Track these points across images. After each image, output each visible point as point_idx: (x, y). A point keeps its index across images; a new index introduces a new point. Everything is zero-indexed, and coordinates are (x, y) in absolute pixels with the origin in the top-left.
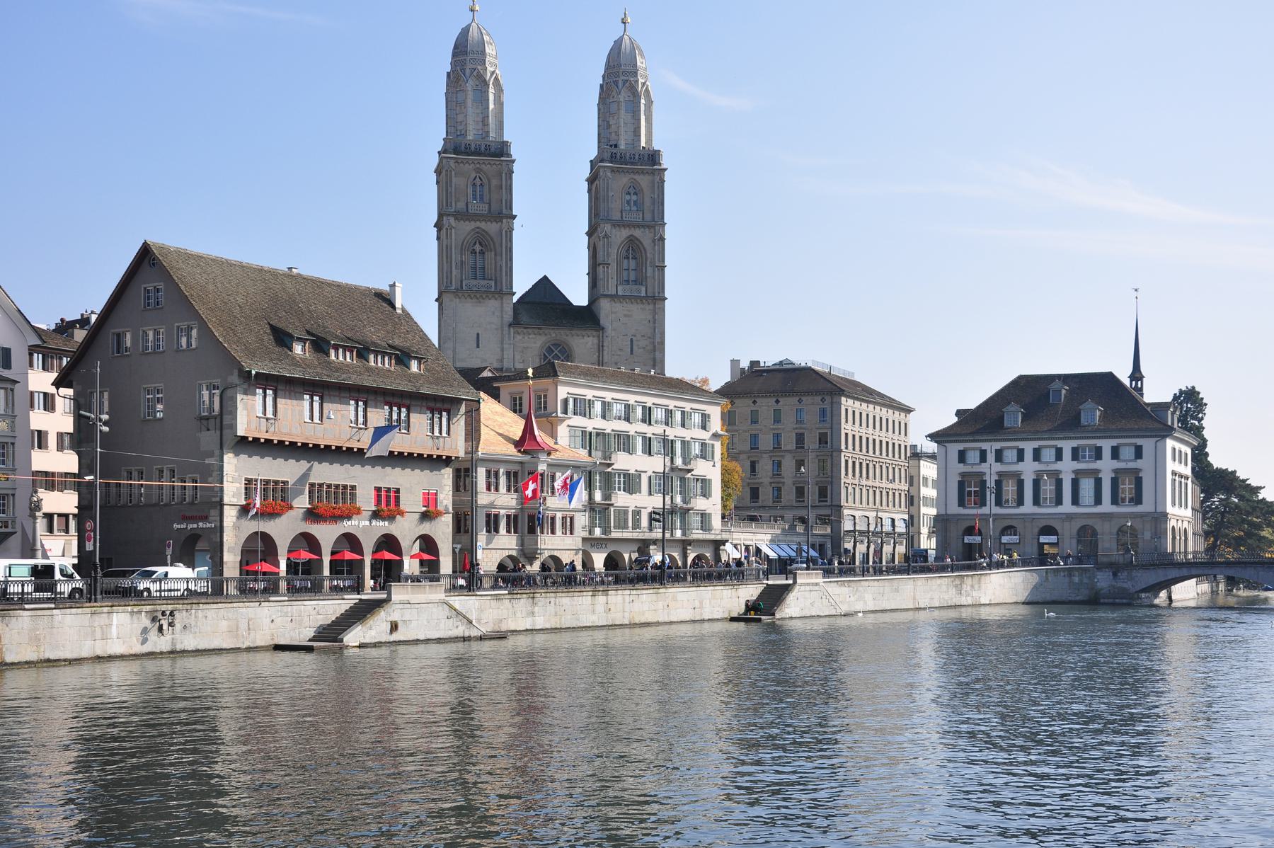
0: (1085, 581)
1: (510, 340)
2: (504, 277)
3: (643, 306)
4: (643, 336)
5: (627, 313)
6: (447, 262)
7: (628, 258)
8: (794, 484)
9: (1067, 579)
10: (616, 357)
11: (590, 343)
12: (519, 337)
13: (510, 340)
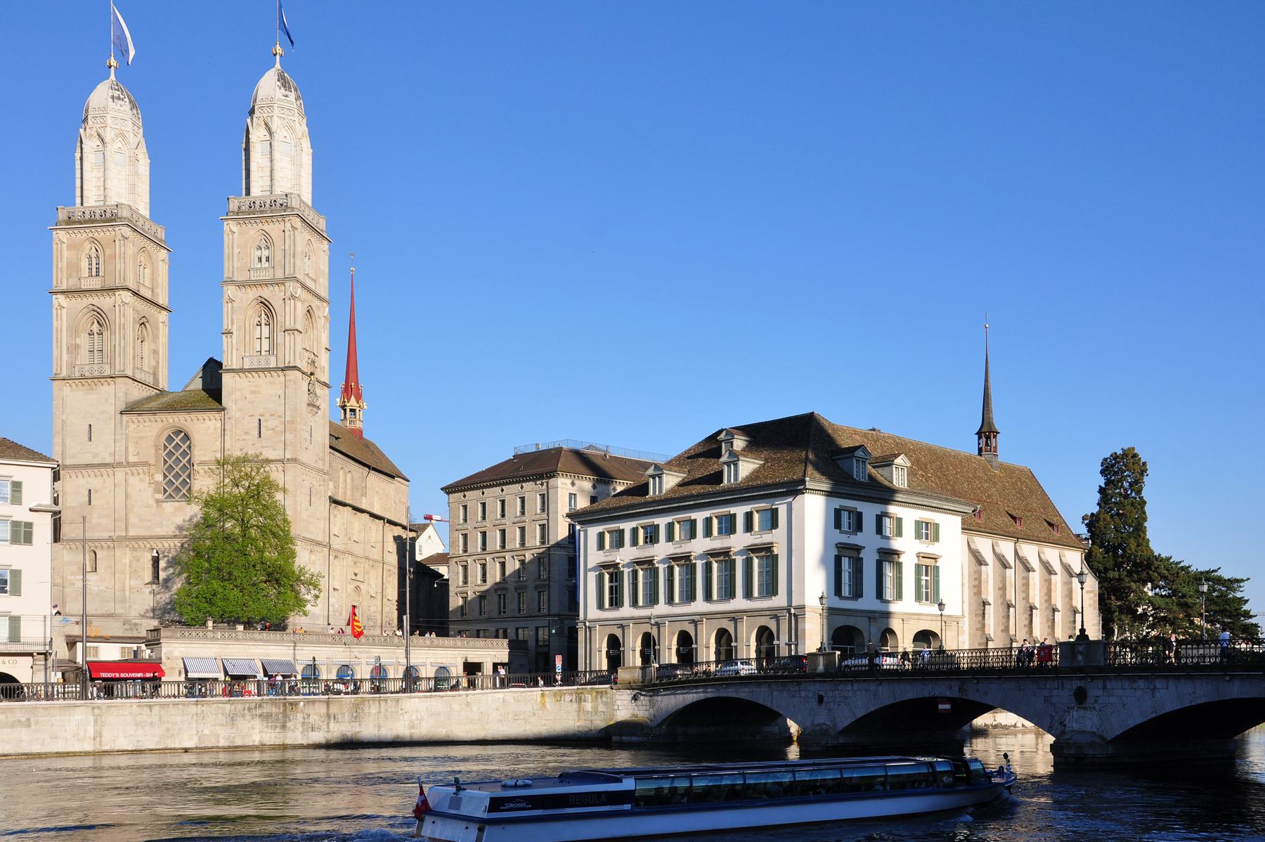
0: (601, 708)
1: (122, 429)
3: (272, 380)
4: (273, 415)
5: (254, 389)
6: (57, 347)
7: (261, 325)
10: (242, 442)
11: (212, 428)
12: (133, 426)
13: (122, 429)
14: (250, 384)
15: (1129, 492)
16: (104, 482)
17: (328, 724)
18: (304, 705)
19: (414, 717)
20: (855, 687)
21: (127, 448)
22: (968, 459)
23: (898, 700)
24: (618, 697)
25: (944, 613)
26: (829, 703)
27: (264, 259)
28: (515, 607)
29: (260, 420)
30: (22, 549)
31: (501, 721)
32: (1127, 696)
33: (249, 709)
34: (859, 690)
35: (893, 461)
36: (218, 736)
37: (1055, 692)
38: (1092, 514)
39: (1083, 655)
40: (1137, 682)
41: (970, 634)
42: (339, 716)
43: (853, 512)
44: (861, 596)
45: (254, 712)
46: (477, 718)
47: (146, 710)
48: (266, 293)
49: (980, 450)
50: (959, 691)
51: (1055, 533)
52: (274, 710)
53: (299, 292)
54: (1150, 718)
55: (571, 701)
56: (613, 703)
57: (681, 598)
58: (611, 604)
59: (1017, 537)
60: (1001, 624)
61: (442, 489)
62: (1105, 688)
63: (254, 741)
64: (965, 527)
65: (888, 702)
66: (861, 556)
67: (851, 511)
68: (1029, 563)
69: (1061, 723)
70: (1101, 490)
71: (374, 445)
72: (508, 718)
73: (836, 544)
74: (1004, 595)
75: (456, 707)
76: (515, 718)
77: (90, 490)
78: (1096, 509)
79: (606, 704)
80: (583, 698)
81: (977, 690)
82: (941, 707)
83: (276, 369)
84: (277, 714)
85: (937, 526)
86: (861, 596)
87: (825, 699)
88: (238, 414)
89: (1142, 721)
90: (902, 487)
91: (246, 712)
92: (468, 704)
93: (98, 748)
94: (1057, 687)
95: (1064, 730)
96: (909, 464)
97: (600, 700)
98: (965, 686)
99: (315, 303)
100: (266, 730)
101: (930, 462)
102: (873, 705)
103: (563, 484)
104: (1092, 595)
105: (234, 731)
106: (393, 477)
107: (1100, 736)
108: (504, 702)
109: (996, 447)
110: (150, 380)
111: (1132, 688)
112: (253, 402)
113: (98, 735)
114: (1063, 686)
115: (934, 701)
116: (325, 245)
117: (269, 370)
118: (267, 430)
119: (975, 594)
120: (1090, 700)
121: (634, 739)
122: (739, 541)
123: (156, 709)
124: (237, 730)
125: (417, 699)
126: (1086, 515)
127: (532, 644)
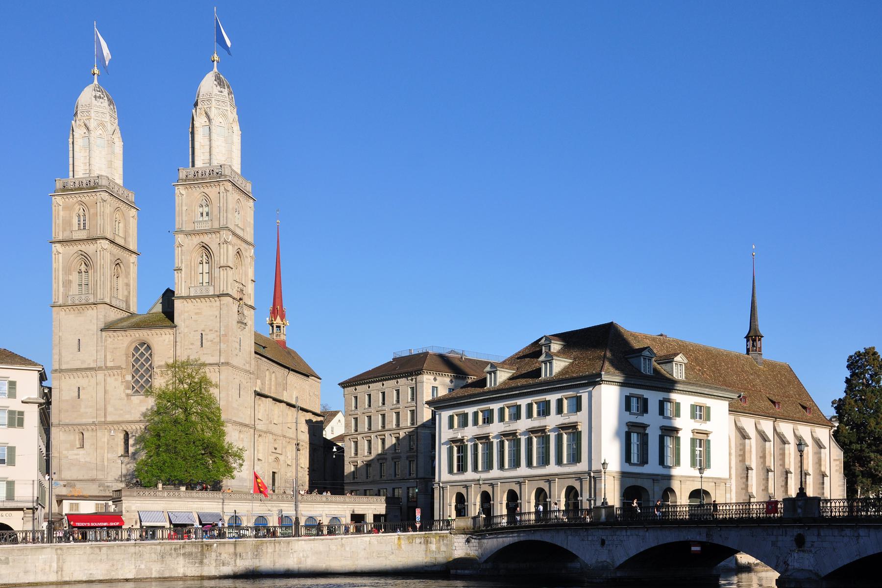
0: (443, 548)
1: (102, 342)
2: (99, 290)
5: (198, 311)
6: (55, 283)
7: (202, 263)
8: (392, 459)
9: (423, 546)
10: (189, 351)
11: (167, 340)
12: (110, 340)
14: (195, 307)
15: (870, 382)
16: (89, 382)
17: (235, 560)
18: (217, 546)
19: (301, 555)
20: (629, 533)
21: (105, 356)
22: (738, 357)
23: (661, 543)
24: (455, 540)
25: (703, 475)
26: (609, 545)
27: (205, 214)
28: (392, 472)
29: (202, 334)
30: (16, 431)
31: (368, 558)
32: (836, 542)
33: (175, 549)
34: (632, 535)
35: (673, 358)
36: (152, 569)
37: (780, 538)
38: (840, 399)
39: (801, 508)
40: (845, 530)
41: (736, 492)
42: (244, 554)
43: (640, 398)
44: (647, 463)
45: (179, 551)
46: (349, 556)
47: (97, 550)
48: (206, 239)
49: (748, 350)
50: (707, 537)
51: (807, 414)
52: (194, 550)
53: (231, 238)
54: (855, 559)
55: (421, 543)
56: (452, 544)
57: (510, 465)
58: (459, 470)
59: (775, 418)
60: (762, 485)
61: (339, 384)
62: (819, 535)
63: (179, 573)
64: (731, 409)
65: (653, 545)
66: (646, 432)
67: (639, 398)
68: (785, 437)
69: (785, 563)
70: (848, 381)
71: (295, 353)
72: (373, 556)
73: (627, 423)
74: (764, 462)
75: (333, 547)
76: (378, 556)
77: (79, 388)
78: (843, 395)
79: (447, 545)
80: (429, 541)
81: (720, 536)
82: (693, 548)
83: (213, 296)
84: (196, 553)
85: (708, 409)
86: (647, 463)
87: (606, 542)
88: (186, 330)
89: (849, 562)
90: (681, 379)
91: (173, 551)
92: (342, 545)
93: (60, 579)
94: (781, 533)
95: (787, 568)
96: (686, 361)
97: (442, 543)
98: (711, 533)
99: (243, 246)
100: (188, 565)
101: (706, 360)
102: (642, 547)
103: (427, 379)
104: (838, 463)
105: (163, 565)
106: (308, 376)
107: (817, 574)
108: (370, 543)
109: (760, 348)
110: (123, 306)
111: (841, 536)
112: (197, 321)
113: (60, 570)
114: (786, 533)
115: (687, 544)
116: (251, 203)
117: (208, 296)
118: (208, 341)
119: (740, 461)
120: (808, 545)
121: (467, 572)
122: (553, 421)
123: (104, 550)
124: (166, 565)
125: (303, 542)
126: (835, 400)
127: (404, 500)
